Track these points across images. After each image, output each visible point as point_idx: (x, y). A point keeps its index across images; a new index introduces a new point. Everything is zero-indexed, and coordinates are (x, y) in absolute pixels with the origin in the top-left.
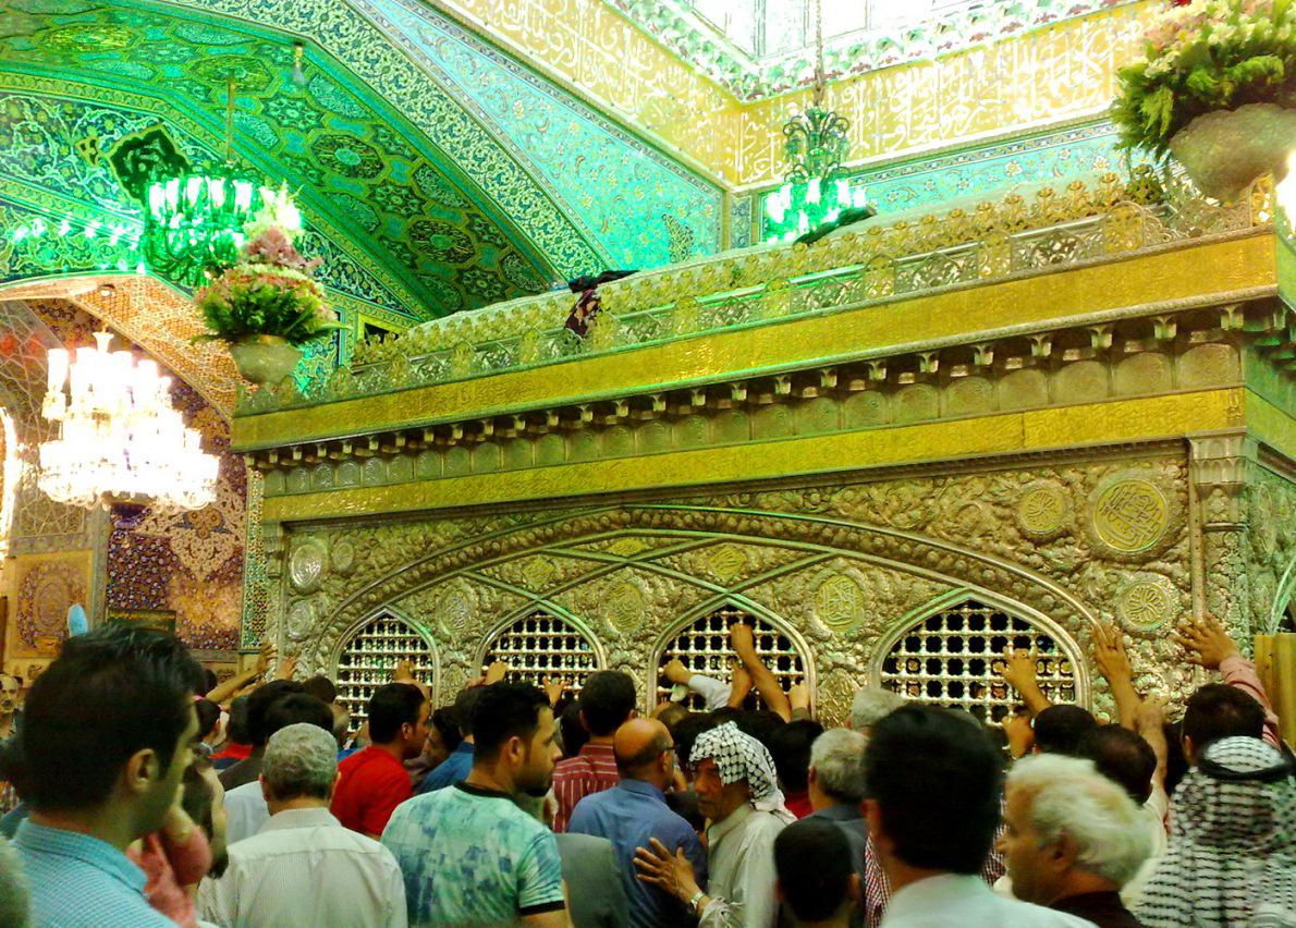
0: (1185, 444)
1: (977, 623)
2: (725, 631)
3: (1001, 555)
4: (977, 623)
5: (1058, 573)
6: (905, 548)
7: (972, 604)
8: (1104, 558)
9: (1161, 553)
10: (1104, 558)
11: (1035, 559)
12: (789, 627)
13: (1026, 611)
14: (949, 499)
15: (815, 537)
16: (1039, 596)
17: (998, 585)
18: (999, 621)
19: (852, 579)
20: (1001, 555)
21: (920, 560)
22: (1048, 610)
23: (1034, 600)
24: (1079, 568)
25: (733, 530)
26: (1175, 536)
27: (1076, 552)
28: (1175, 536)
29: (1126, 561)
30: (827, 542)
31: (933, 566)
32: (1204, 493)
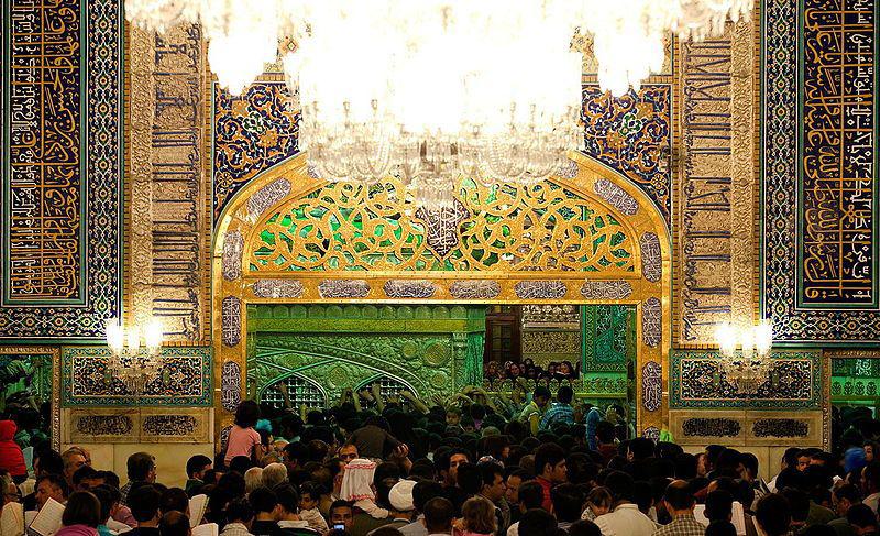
1: (385, 384)
3: (396, 363)
4: (385, 384)
5: (413, 369)
7: (384, 378)
8: (429, 366)
9: (444, 365)
10: (429, 366)
14: (376, 343)
18: (392, 383)
20: (396, 363)
21: (368, 363)
22: (409, 380)
26: (447, 361)
27: (419, 363)
29: (434, 367)
30: (335, 355)
31: (373, 365)
32: (456, 349)
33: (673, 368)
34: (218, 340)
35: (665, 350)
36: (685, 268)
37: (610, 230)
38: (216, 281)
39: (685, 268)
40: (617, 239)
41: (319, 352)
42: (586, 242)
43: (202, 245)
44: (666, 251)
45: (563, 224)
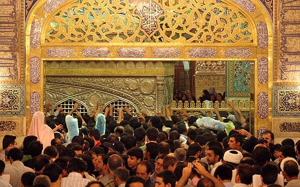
0: (156, 77)
2: (73, 104)
5: (134, 95)
6: (108, 90)
8: (143, 94)
11: (132, 93)
12: (84, 104)
13: (127, 101)
14: (116, 82)
15: (90, 87)
16: (131, 100)
17: (125, 97)
19: (98, 95)
20: (126, 93)
21: (111, 92)
22: (133, 102)
23: (131, 100)
24: (139, 95)
25: (72, 85)
26: (153, 91)
28: (153, 91)
29: (146, 95)
30: (93, 88)
32: (158, 85)
33: (274, 94)
34: (27, 79)
35: (270, 85)
36: (281, 41)
37: (240, 20)
38: (28, 49)
39: (281, 41)
40: (245, 25)
41: (84, 86)
42: (228, 27)
43: (19, 29)
44: (270, 31)
45: (214, 18)
